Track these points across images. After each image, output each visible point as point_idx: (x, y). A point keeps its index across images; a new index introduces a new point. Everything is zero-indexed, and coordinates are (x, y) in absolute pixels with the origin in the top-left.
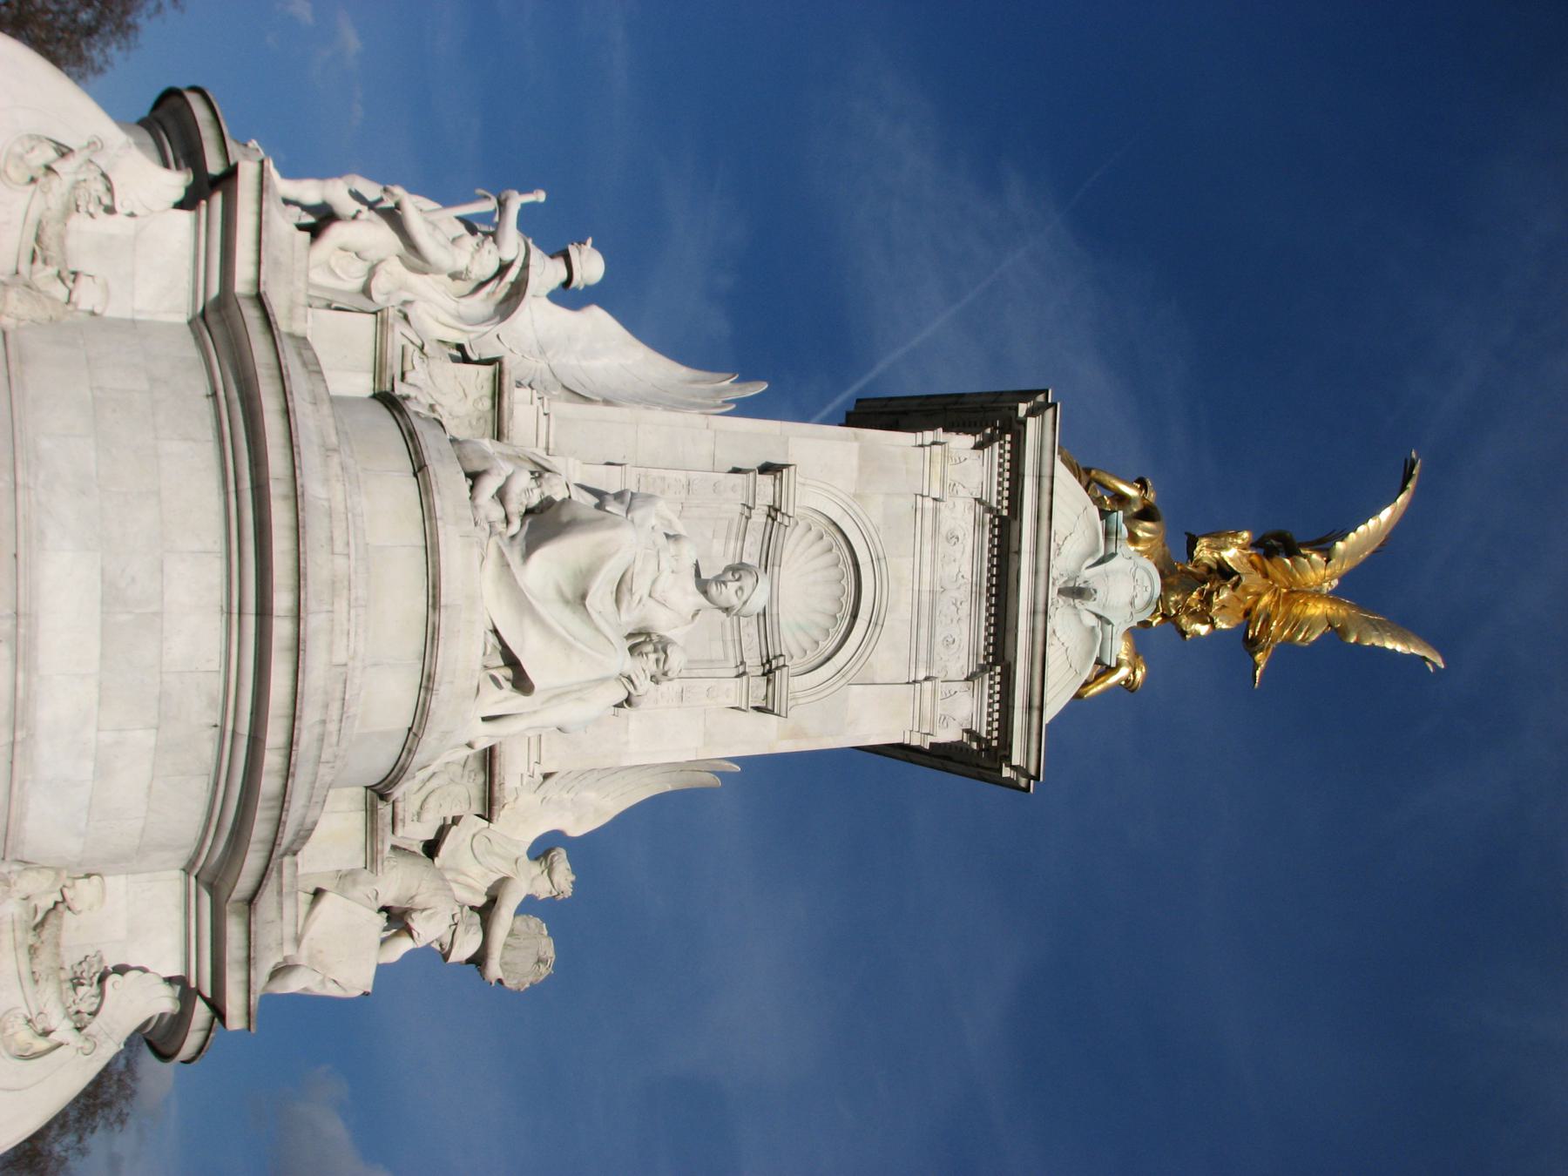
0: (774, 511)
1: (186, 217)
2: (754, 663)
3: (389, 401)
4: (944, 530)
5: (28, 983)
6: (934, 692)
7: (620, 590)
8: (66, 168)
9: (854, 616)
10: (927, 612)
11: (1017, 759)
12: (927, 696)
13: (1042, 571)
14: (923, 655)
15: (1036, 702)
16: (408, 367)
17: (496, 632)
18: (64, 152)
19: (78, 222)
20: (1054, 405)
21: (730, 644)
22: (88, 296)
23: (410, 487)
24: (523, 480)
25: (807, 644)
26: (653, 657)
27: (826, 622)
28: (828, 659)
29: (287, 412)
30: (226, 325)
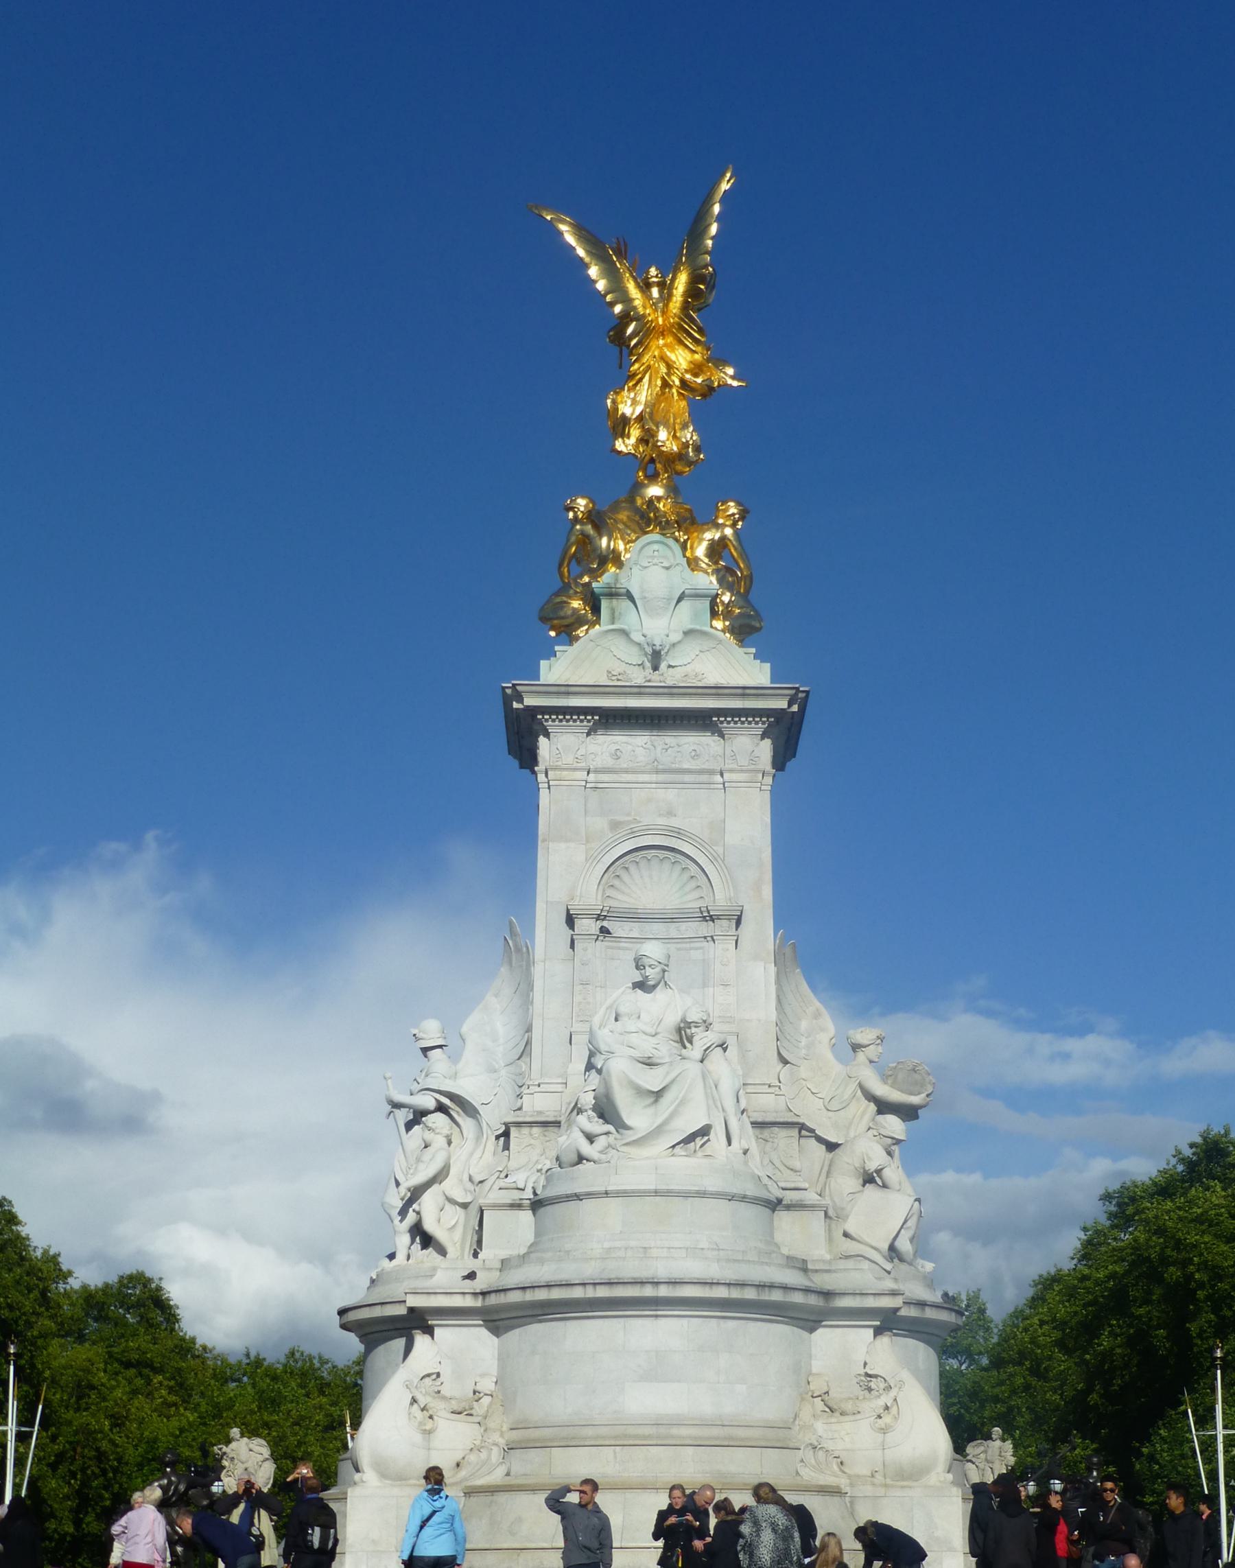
1: (437, 1331)
2: (705, 928)
3: (537, 1205)
5: (858, 1416)
6: (731, 771)
7: (649, 1063)
8: (422, 1401)
9: (673, 850)
10: (672, 774)
11: (783, 704)
12: (734, 776)
13: (640, 691)
14: (704, 778)
15: (740, 691)
16: (514, 1185)
17: (673, 1147)
18: (414, 1401)
19: (446, 1391)
20: (514, 685)
21: (693, 945)
22: (487, 1385)
23: (587, 1204)
24: (582, 1120)
25: (693, 884)
26: (694, 1030)
27: (678, 868)
28: (703, 870)
29: (549, 1286)
30: (499, 1316)
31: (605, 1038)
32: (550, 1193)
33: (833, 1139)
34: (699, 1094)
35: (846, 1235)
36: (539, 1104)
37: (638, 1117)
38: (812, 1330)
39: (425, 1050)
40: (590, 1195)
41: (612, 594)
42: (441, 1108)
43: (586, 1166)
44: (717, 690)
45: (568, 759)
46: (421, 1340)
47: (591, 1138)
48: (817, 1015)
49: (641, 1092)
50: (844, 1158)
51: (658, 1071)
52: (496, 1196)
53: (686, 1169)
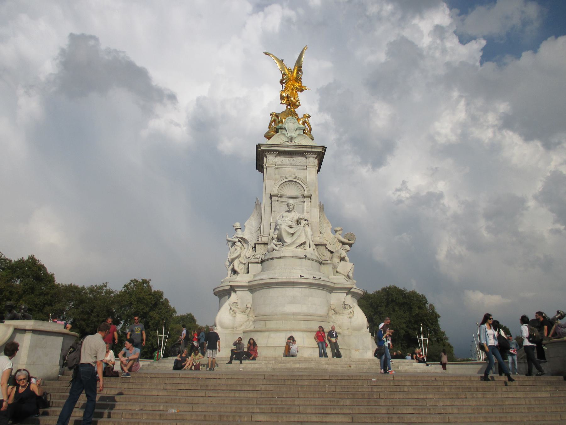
0: (278, 197)
1: (237, 292)
3: (262, 262)
4: (280, 163)
8: (233, 308)
10: (295, 166)
13: (288, 146)
18: (231, 309)
19: (239, 306)
22: (249, 305)
23: (275, 260)
24: (274, 241)
31: (280, 222)
32: (266, 258)
33: (332, 250)
34: (303, 234)
35: (337, 272)
36: (264, 239)
37: (288, 240)
38: (331, 293)
39: (236, 229)
40: (276, 258)
41: (281, 128)
42: (239, 241)
43: (275, 251)
44: (306, 146)
45: (271, 162)
46: (233, 294)
47: (276, 245)
48: (328, 223)
49: (289, 233)
50: (335, 255)
51: (292, 229)
52: (253, 260)
53: (300, 252)
